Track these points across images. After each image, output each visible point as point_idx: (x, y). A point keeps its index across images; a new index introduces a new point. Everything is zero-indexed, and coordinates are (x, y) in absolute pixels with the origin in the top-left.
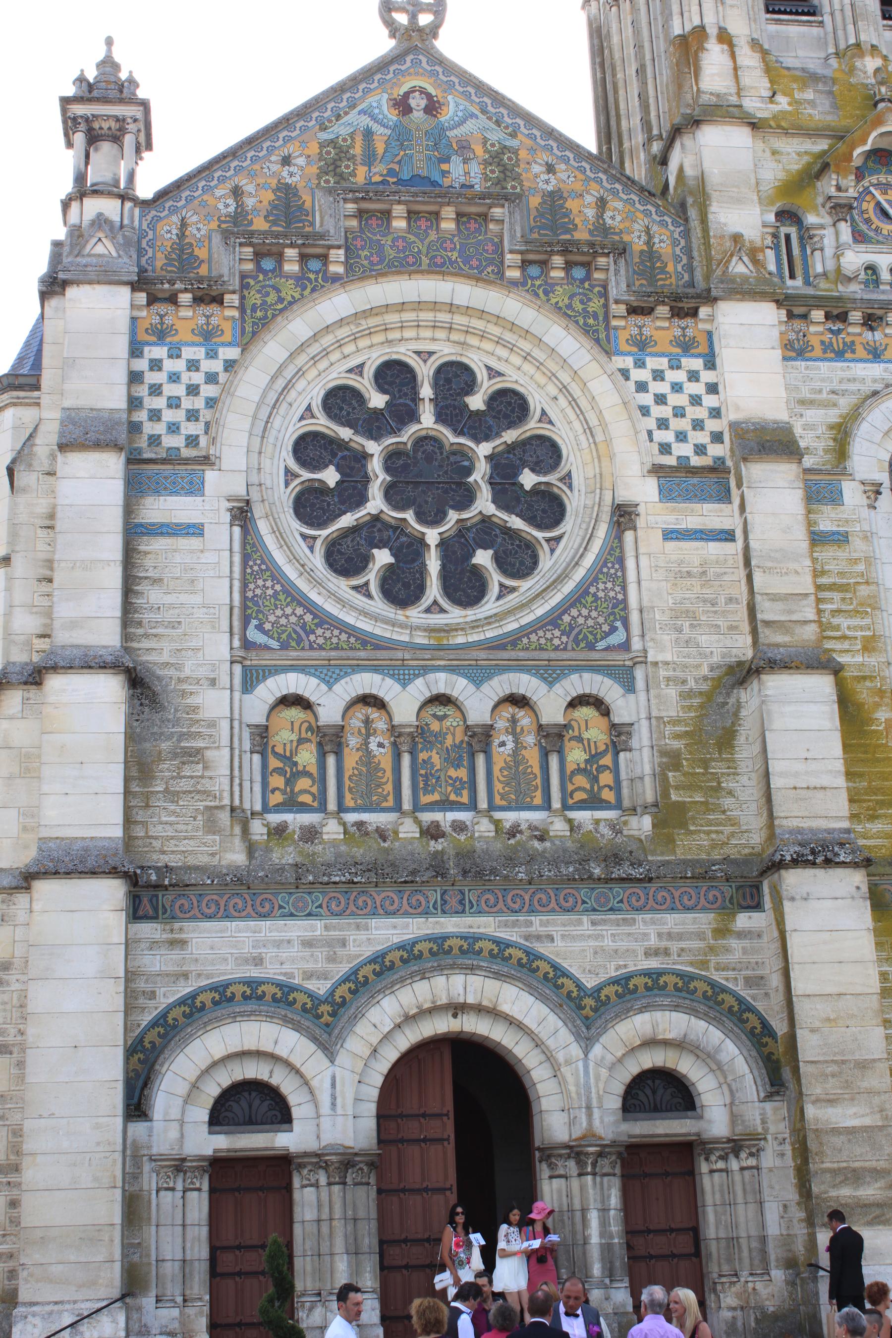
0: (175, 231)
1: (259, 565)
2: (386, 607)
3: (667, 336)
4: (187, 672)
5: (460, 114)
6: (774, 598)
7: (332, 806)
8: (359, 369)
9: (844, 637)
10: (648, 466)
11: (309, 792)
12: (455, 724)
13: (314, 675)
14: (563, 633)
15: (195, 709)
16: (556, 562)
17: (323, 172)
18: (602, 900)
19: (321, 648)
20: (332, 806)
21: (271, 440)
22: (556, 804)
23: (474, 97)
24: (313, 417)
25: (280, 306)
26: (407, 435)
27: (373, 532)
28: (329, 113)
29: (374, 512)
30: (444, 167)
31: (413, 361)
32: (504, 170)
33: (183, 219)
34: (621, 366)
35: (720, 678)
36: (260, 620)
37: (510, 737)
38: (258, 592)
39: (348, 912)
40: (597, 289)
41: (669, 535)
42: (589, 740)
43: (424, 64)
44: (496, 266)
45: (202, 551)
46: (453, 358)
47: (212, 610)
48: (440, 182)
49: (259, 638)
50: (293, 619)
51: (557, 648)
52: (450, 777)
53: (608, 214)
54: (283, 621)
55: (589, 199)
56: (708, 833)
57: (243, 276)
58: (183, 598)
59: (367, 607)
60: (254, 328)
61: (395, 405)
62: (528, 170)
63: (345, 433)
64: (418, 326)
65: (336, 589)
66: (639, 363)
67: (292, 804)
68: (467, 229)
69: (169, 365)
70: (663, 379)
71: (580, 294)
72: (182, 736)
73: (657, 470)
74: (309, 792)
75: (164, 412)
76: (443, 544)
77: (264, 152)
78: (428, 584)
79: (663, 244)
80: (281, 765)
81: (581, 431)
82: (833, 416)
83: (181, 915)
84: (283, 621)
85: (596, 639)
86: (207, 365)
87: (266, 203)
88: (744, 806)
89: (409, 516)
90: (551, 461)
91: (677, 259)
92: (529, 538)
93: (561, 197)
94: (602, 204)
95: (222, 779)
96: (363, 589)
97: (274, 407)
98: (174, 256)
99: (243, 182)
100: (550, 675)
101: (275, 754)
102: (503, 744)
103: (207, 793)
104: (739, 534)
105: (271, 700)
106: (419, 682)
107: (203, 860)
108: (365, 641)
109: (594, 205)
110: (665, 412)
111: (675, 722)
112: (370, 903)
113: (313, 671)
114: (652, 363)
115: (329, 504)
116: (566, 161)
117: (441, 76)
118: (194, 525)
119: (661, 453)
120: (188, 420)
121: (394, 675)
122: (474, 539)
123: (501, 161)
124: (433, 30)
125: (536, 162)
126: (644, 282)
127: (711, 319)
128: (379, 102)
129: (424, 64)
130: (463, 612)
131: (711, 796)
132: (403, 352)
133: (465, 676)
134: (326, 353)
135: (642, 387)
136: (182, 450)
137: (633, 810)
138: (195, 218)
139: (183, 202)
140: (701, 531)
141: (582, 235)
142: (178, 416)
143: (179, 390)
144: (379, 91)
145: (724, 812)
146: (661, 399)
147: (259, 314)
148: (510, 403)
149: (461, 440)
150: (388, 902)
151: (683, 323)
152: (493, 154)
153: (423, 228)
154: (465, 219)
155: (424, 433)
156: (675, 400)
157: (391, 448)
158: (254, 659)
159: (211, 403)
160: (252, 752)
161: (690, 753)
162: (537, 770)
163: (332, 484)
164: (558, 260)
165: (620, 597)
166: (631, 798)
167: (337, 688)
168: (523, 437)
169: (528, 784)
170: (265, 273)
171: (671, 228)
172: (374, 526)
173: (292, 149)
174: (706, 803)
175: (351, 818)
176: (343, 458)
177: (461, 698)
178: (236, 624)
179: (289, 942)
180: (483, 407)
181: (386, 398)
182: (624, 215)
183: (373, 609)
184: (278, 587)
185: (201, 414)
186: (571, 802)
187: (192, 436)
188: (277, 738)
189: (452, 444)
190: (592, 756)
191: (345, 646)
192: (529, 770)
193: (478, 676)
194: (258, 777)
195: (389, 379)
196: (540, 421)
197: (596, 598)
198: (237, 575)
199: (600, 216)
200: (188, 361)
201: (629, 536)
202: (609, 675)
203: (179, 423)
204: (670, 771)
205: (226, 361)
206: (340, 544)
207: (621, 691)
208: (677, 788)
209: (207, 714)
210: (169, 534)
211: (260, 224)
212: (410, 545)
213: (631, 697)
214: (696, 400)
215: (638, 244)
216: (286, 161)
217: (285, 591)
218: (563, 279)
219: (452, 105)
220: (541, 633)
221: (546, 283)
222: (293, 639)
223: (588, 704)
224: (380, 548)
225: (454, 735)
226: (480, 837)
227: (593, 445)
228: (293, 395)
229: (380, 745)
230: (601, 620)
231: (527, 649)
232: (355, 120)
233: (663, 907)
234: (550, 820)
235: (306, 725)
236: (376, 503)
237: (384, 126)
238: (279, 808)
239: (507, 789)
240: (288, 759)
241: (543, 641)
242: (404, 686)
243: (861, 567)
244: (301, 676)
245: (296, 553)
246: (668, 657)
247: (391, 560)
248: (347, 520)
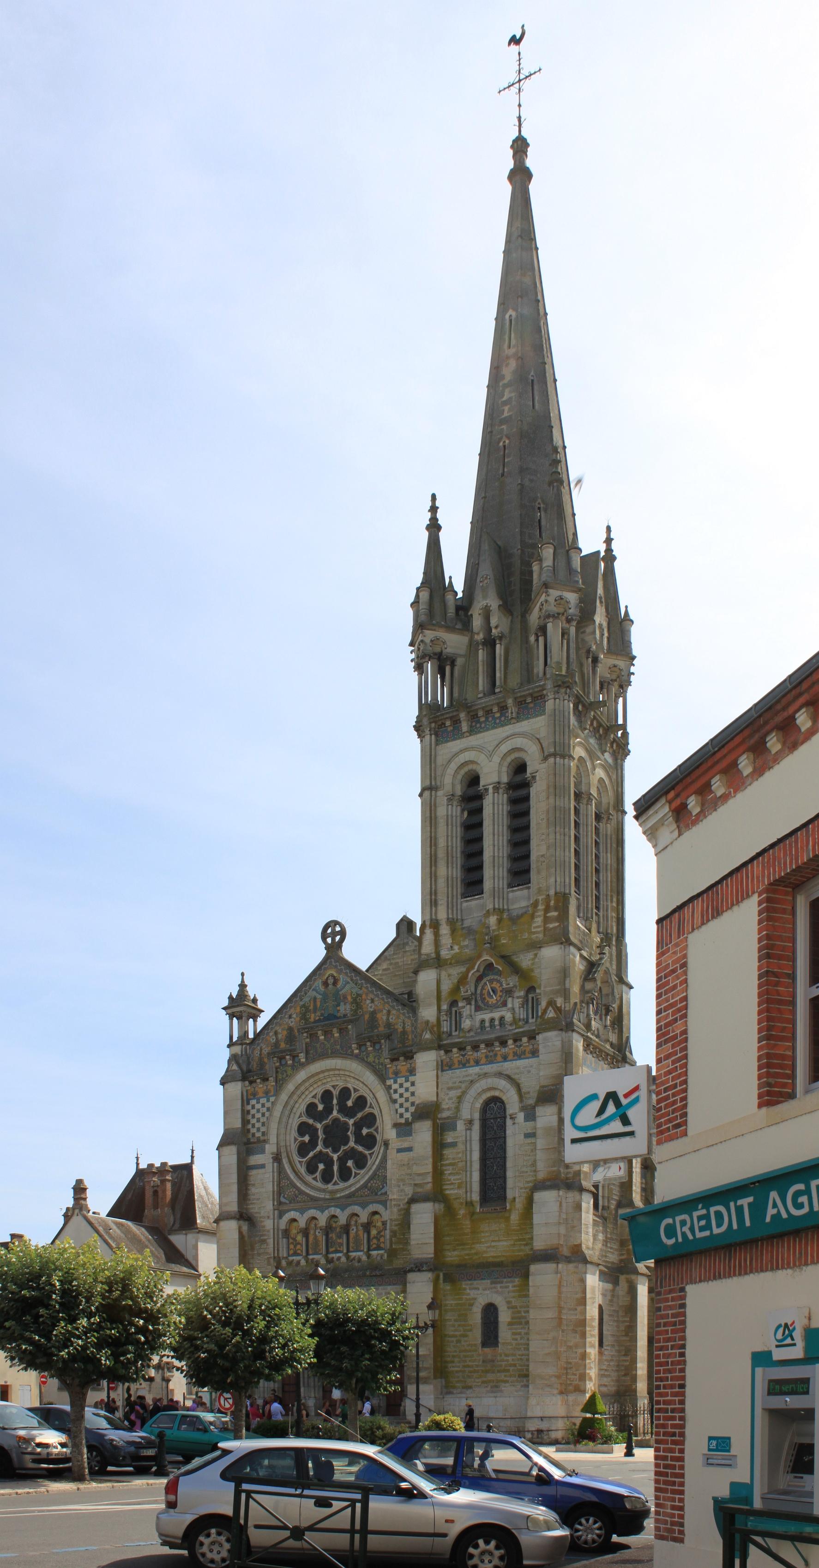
3: (405, 1068)
4: (262, 1214)
6: (419, 1175)
7: (304, 1254)
9: (452, 1184)
15: (264, 1227)
17: (301, 1019)
31: (332, 1089)
41: (399, 1151)
55: (385, 1011)
57: (277, 1068)
67: (295, 1254)
69: (258, 1106)
73: (396, 1125)
76: (339, 1158)
79: (408, 1028)
82: (458, 1092)
94: (389, 1012)
96: (315, 1179)
103: (267, 1253)
110: (402, 1100)
111: (395, 1220)
114: (399, 1081)
116: (377, 996)
123: (357, 1002)
124: (339, 945)
143: (259, 1115)
164: (368, 1044)
193: (343, 1208)
194: (285, 1246)
199: (388, 1019)
211: (283, 1045)
216: (290, 1017)
228: (295, 1109)
236: (320, 1147)
238: (293, 1255)
240: (294, 1239)
243: (460, 1155)
246: (395, 1197)
248: (311, 1154)
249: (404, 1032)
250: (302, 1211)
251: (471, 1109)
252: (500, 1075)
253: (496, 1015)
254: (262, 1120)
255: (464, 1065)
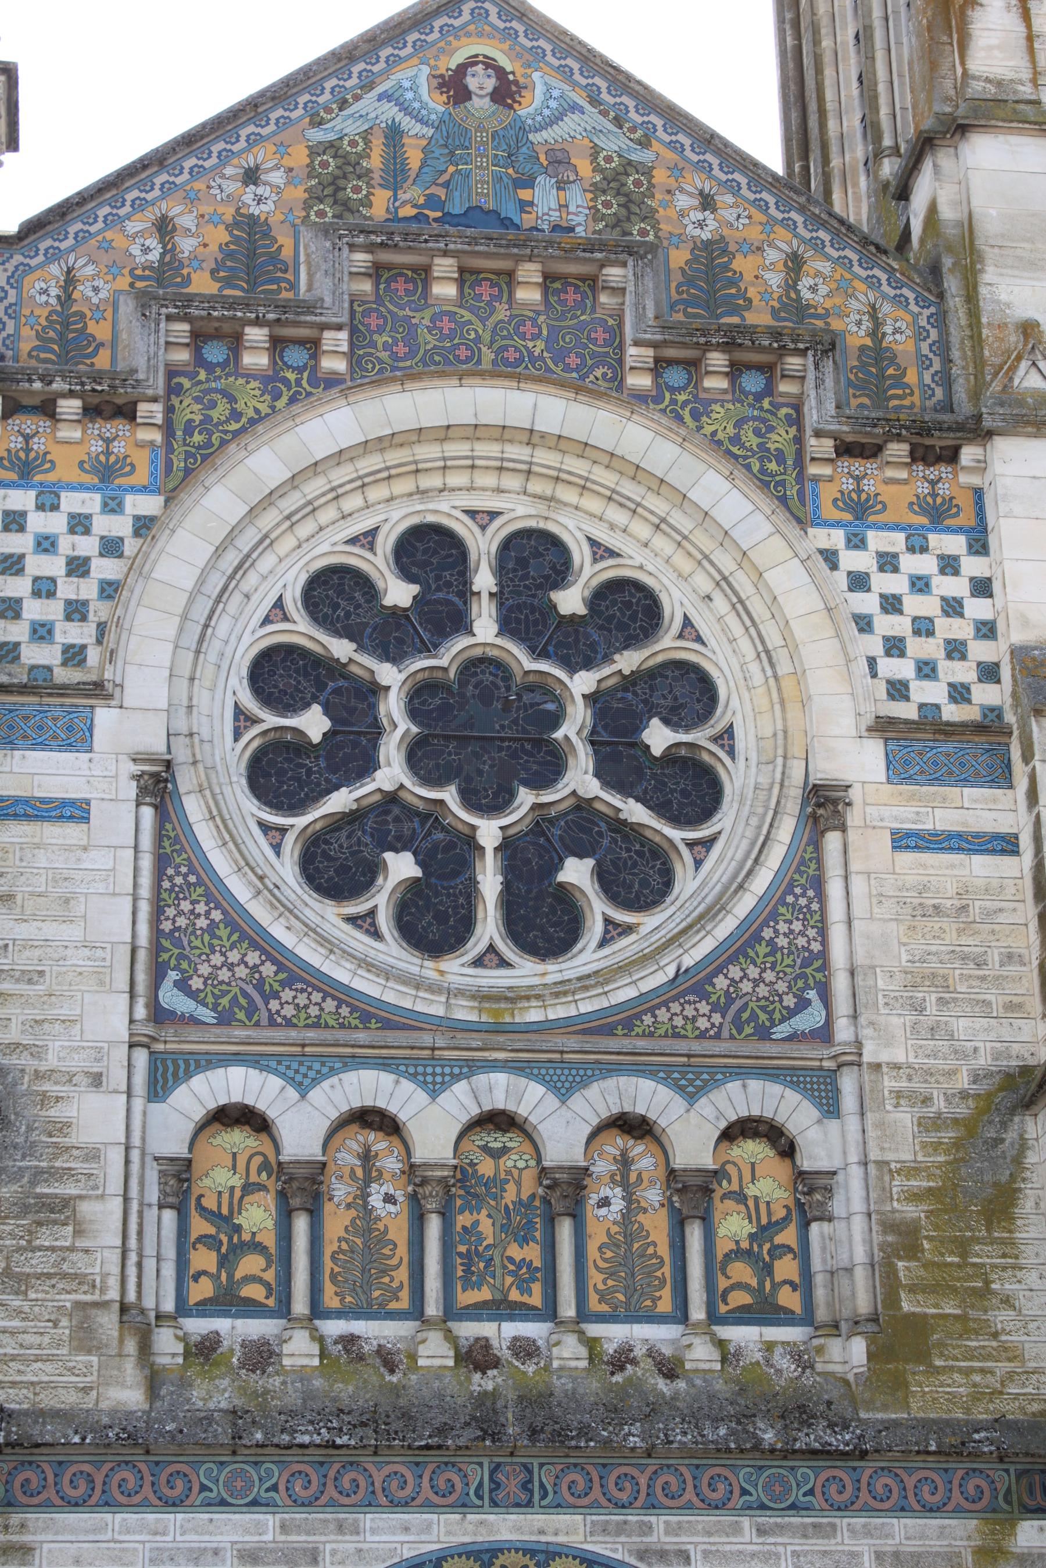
0: (54, 292)
1: (185, 876)
2: (404, 955)
3: (907, 494)
4: (51, 1061)
5: (553, 104)
7: (300, 1306)
8: (368, 539)
10: (869, 720)
11: (260, 1281)
12: (521, 1164)
13: (276, 1072)
14: (715, 1008)
15: (64, 1127)
16: (704, 884)
17: (314, 197)
18: (778, 1489)
19: (289, 1023)
20: (300, 1306)
21: (212, 657)
22: (698, 1313)
23: (577, 77)
24: (286, 618)
25: (234, 426)
26: (450, 655)
27: (386, 822)
28: (327, 96)
29: (388, 787)
30: (524, 194)
31: (463, 528)
32: (628, 202)
33: (69, 271)
34: (824, 545)
35: (989, 1095)
36: (183, 971)
37: (618, 1190)
38: (182, 922)
39: (323, 1500)
40: (784, 411)
41: (904, 841)
42: (756, 1198)
43: (493, 18)
44: (611, 367)
45: (85, 849)
46: (532, 523)
47: (99, 953)
48: (517, 221)
49: (183, 1004)
50: (242, 972)
51: (703, 1035)
52: (511, 1260)
53: (805, 283)
54: (224, 975)
55: (772, 255)
56: (967, 1372)
57: (172, 372)
58: (50, 930)
59: (372, 953)
60: (186, 463)
61: (428, 603)
62: (667, 205)
63: (341, 649)
64: (473, 467)
65: (317, 920)
66: (855, 541)
67: (228, 1301)
68: (562, 302)
69: (38, 522)
70: (896, 570)
71: (754, 419)
72: (38, 1175)
73: (884, 727)
74: (260, 1281)
75: (26, 604)
76: (507, 847)
77: (214, 160)
78: (480, 915)
80: (212, 1230)
81: (751, 655)
83: (24, 1500)
84: (224, 975)
85: (772, 1020)
86: (104, 525)
87: (214, 248)
88: (1032, 1326)
89: (449, 795)
90: (698, 707)
91: (924, 363)
92: (657, 839)
93: (725, 251)
94: (795, 264)
95: (106, 1253)
96: (366, 922)
97: (218, 600)
98: (52, 334)
99: (174, 209)
100: (691, 1082)
101: (202, 1210)
102: (605, 1202)
103: (79, 1278)
104: (1026, 842)
105: (199, 1114)
106: (461, 1088)
107: (69, 1399)
108: (368, 1013)
109: (780, 266)
110: (900, 625)
111: (911, 1171)
112: (362, 1484)
113: (273, 1064)
115: (309, 772)
116: (734, 189)
117: (522, 39)
118: (72, 803)
119: (891, 697)
120: (68, 618)
121: (415, 1075)
122: (561, 838)
123: (623, 189)
125: (682, 190)
126: (866, 401)
127: (982, 467)
128: (413, 79)
129: (493, 18)
130: (541, 968)
131: (972, 1307)
132: (446, 511)
133: (542, 1081)
134: (311, 508)
135: (859, 582)
136: (56, 670)
137: (835, 1327)
138: (90, 270)
139: (70, 242)
140: (960, 835)
141: (759, 317)
142: (52, 610)
143: (54, 566)
144: (415, 61)
145: (995, 1335)
146: (891, 604)
147: (197, 438)
148: (628, 605)
149: (544, 666)
150: (394, 1484)
151: (932, 472)
152: (609, 174)
153: (486, 298)
154: (557, 285)
155: (478, 652)
156: (915, 605)
157: (420, 676)
158: (171, 1042)
159: (109, 591)
160: (161, 1207)
161: (937, 1228)
162: (664, 1250)
163: (316, 737)
164: (717, 360)
165: (816, 947)
166: (830, 1305)
167: (316, 1095)
168: (651, 663)
169: (649, 1274)
170: (210, 367)
171: (916, 309)
172: (387, 812)
173: (262, 155)
174: (963, 1318)
175: (333, 1328)
176: (337, 691)
177: (533, 1119)
178: (142, 977)
179: (216, 1552)
180: (581, 610)
181: (415, 589)
182: (834, 286)
183: (382, 957)
184: (217, 915)
185: (91, 608)
186: (723, 1309)
187: (73, 646)
188: (207, 1182)
189: (527, 673)
190: (763, 1229)
191: (331, 1022)
192: (651, 1250)
193: (565, 1079)
194: (170, 1252)
195: (419, 556)
196: (681, 636)
197: (774, 949)
198: (145, 892)
199: (791, 285)
200: (72, 516)
201: (832, 841)
202: (794, 1085)
203: (52, 623)
204: (900, 1258)
205: (137, 518)
206: (327, 842)
207: (815, 1113)
208: (912, 1289)
209: (83, 1136)
210: (27, 817)
211: (203, 284)
212: (450, 846)
213: (833, 1125)
214: (953, 607)
215: (856, 334)
216: (251, 176)
217: (230, 923)
218: (725, 391)
219: (539, 89)
220: (675, 1007)
221: (696, 396)
222: (241, 1008)
223: (755, 1135)
224: (397, 851)
225: (518, 1184)
226: (561, 1368)
227: (772, 681)
228: (252, 579)
229: (389, 1199)
230: (781, 987)
231: (651, 1035)
232: (374, 110)
233: (887, 1505)
234: (685, 1341)
235: (258, 1160)
236: (392, 772)
237: (421, 121)
238: (206, 1308)
239: (610, 1283)
240: (225, 1220)
241: (679, 1021)
242: (434, 1094)
244: (252, 1071)
245: (250, 856)
246: (901, 1058)
247: (416, 872)
248: (340, 801)
249: (878, 354)
254: (67, 589)
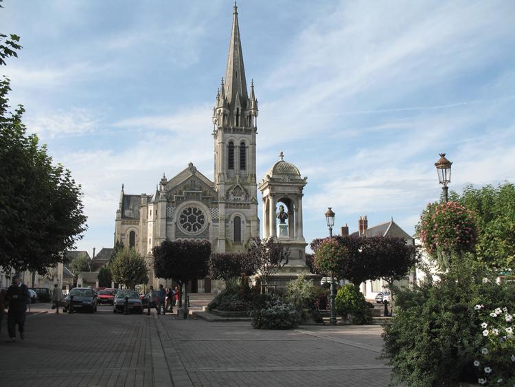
245: (180, 227)
250: (183, 238)
251: (232, 219)
252: (239, 212)
253: (239, 198)
255: (231, 208)
